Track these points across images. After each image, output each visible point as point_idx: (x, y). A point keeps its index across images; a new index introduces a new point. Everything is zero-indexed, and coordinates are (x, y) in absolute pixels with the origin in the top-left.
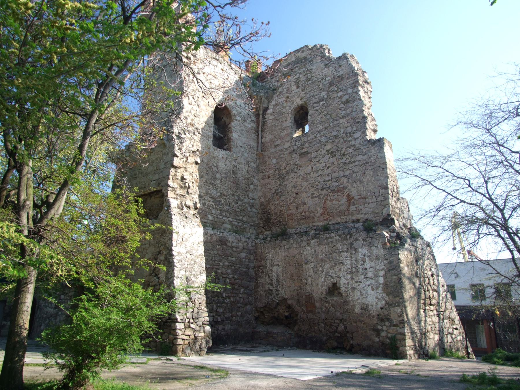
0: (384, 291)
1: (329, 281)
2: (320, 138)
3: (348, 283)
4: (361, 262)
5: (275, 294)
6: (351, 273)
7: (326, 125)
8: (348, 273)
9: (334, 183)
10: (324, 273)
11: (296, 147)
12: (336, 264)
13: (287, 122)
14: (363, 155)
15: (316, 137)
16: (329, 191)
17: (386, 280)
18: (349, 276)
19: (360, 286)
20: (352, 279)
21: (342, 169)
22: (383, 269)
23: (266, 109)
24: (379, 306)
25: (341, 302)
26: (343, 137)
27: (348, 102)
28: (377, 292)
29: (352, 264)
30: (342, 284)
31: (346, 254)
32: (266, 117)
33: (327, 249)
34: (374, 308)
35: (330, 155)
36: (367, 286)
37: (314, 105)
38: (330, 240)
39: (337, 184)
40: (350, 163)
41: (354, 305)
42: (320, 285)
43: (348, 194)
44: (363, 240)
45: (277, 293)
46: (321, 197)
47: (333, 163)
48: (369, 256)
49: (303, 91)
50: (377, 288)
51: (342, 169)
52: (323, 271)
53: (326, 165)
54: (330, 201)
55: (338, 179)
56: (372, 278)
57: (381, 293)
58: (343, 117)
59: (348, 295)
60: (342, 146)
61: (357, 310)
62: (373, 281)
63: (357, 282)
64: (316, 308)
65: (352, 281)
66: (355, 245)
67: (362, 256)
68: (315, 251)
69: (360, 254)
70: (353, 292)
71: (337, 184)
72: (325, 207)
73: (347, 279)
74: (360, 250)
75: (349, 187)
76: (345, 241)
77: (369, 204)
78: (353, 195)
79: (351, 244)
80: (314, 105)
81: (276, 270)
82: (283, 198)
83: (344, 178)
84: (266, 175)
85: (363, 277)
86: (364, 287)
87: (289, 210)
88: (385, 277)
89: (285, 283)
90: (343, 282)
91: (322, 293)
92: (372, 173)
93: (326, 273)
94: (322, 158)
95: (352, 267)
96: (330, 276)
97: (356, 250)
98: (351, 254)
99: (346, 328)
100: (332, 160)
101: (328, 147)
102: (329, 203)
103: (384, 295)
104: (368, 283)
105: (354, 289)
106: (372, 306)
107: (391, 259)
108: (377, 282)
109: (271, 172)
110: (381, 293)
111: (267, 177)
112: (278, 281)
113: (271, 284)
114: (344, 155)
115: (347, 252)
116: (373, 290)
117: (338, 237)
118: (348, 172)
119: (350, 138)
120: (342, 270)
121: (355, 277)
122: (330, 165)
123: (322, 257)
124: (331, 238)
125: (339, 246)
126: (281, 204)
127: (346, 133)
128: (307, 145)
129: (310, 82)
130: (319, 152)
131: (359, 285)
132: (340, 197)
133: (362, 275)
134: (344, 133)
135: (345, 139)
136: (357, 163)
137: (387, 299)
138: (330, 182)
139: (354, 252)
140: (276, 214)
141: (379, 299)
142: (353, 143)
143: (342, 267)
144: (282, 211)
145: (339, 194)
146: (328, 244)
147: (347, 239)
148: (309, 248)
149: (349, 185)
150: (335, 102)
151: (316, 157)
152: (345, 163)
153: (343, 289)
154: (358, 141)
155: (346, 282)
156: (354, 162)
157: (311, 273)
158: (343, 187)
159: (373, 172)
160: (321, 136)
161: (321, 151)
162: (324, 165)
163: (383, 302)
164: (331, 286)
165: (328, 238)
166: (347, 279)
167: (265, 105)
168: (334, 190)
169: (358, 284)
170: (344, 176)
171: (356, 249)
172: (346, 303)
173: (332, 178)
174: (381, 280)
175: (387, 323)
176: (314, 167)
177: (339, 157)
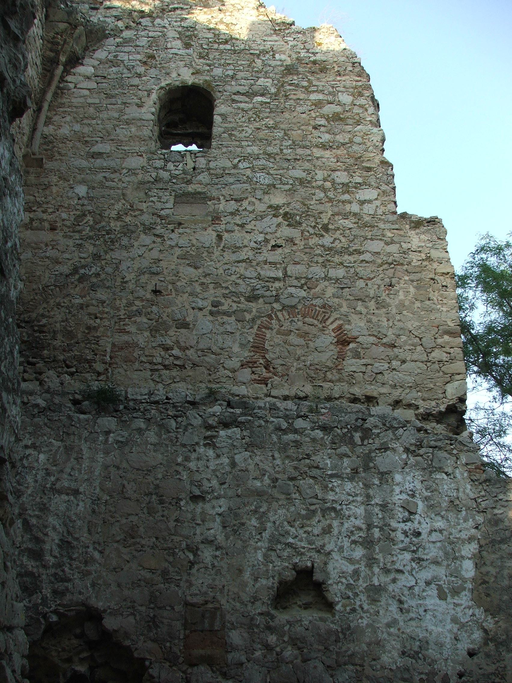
0: (478, 601)
1: (282, 566)
2: (248, 172)
3: (356, 573)
4: (401, 514)
5: (47, 591)
6: (368, 543)
7: (270, 149)
8: (354, 542)
9: (292, 290)
10: (266, 535)
11: (165, 175)
12: (314, 512)
13: (143, 110)
14: (387, 244)
15: (235, 167)
16: (276, 306)
17: (484, 569)
18: (359, 553)
19: (400, 584)
20: (371, 561)
21: (321, 260)
22: (471, 539)
23: (75, 61)
24: (464, 646)
25: (329, 632)
26: (324, 190)
27: (337, 118)
28: (456, 605)
29: (368, 515)
30: (334, 575)
31: (349, 486)
32: (69, 78)
33: (278, 462)
34: (446, 653)
35: (280, 219)
36: (422, 584)
37: (236, 97)
38: (291, 437)
39: (303, 294)
40: (345, 251)
41: (378, 643)
42: (247, 575)
43: (340, 327)
44: (407, 450)
45: (61, 586)
46: (248, 317)
47: (291, 241)
48: (427, 499)
49: (201, 57)
50: (456, 592)
51: (321, 260)
52: (261, 530)
53: (267, 241)
54: (278, 333)
55: (307, 283)
56: (436, 563)
57: (469, 608)
58: (324, 146)
59: (354, 610)
60: (321, 208)
61: (391, 657)
62: (441, 571)
63: (387, 571)
64: (228, 648)
65: (369, 566)
66: (383, 461)
67: (404, 496)
68: (233, 464)
69: (397, 489)
70: (374, 601)
71: (303, 294)
72: (259, 347)
74: (398, 478)
75: (344, 309)
76: (344, 449)
77: (404, 362)
78: (355, 334)
79: (368, 459)
80: (236, 97)
81: (63, 507)
82: (102, 294)
83: (326, 283)
84: (41, 220)
85: (408, 556)
86: (411, 588)
87: (123, 331)
88: (479, 560)
89: (97, 555)
90: (339, 566)
91: (255, 599)
92: (412, 290)
93: (272, 536)
94: (256, 219)
95: (370, 526)
96: (289, 545)
97: (385, 476)
98: (367, 486)
100: (286, 232)
101: (278, 199)
102: (272, 338)
103: (479, 612)
104: (426, 575)
105: (375, 592)
106: (440, 645)
107: (496, 511)
108: (456, 573)
109: (64, 216)
110: (469, 608)
111: (47, 225)
112: (65, 545)
113: (37, 555)
114: (325, 228)
115: (351, 479)
116: (442, 596)
117: (319, 434)
118: (340, 273)
119: (346, 197)
120: (335, 531)
121: (380, 557)
122: (279, 242)
123: (259, 484)
124: (296, 431)
125: (325, 460)
126: (92, 310)
127: (333, 182)
128: (204, 177)
129: (228, 47)
130: (245, 204)
131: (394, 581)
132: (314, 330)
133: (404, 549)
134: (325, 180)
135: (331, 194)
136: (367, 257)
137: (490, 624)
138: (277, 284)
139: (376, 481)
140: (69, 334)
141: (463, 626)
142: (355, 208)
143: (335, 523)
144: (96, 329)
145: (308, 320)
146: (283, 448)
147: (351, 443)
148: (211, 453)
149: (344, 304)
150: (299, 109)
151: (232, 214)
152: (330, 249)
153: (335, 591)
154: (368, 209)
155: (350, 568)
156: (359, 253)
157: (215, 529)
158: (324, 307)
159: (417, 288)
160: (252, 169)
161: (251, 203)
162: (261, 238)
163: (477, 635)
164: (290, 575)
165: (285, 432)
166: (351, 561)
167: (78, 49)
168: (294, 307)
169: (392, 576)
170: (326, 278)
171: (382, 474)
172: (348, 632)
173: (286, 275)
174: (468, 569)
176: (226, 236)
177: (312, 231)
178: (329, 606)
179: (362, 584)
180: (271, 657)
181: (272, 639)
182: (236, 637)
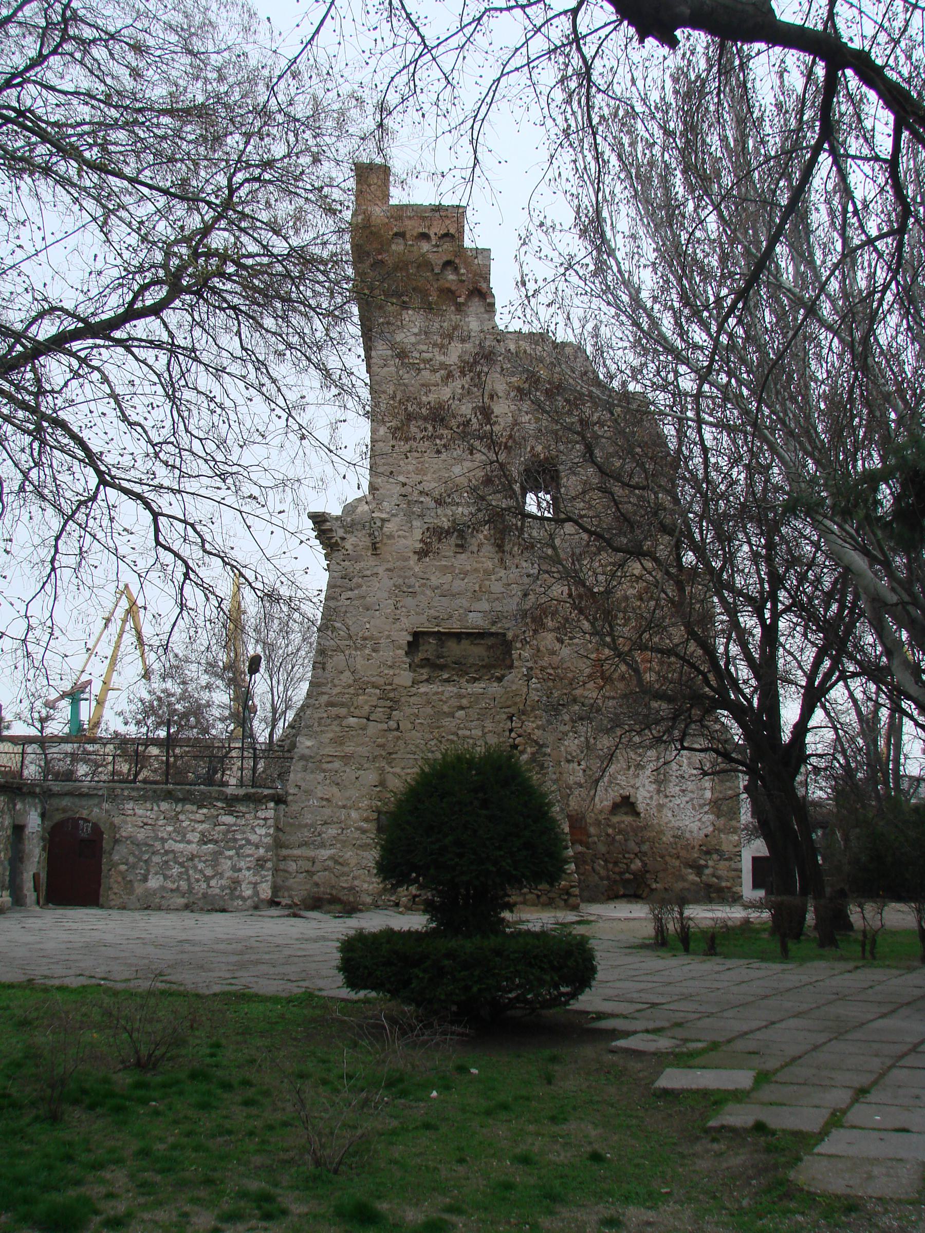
3: (651, 798)
25: (638, 827)
30: (640, 799)
61: (667, 838)
63: (666, 797)
64: (589, 836)
70: (659, 811)
73: (649, 792)
99: (645, 864)
105: (660, 807)
106: (691, 832)
153: (641, 807)
155: (648, 795)
164: (618, 799)
166: (649, 792)
175: (715, 857)
178: (638, 814)
179: (654, 803)
180: (610, 839)
181: (610, 831)
182: (592, 830)
